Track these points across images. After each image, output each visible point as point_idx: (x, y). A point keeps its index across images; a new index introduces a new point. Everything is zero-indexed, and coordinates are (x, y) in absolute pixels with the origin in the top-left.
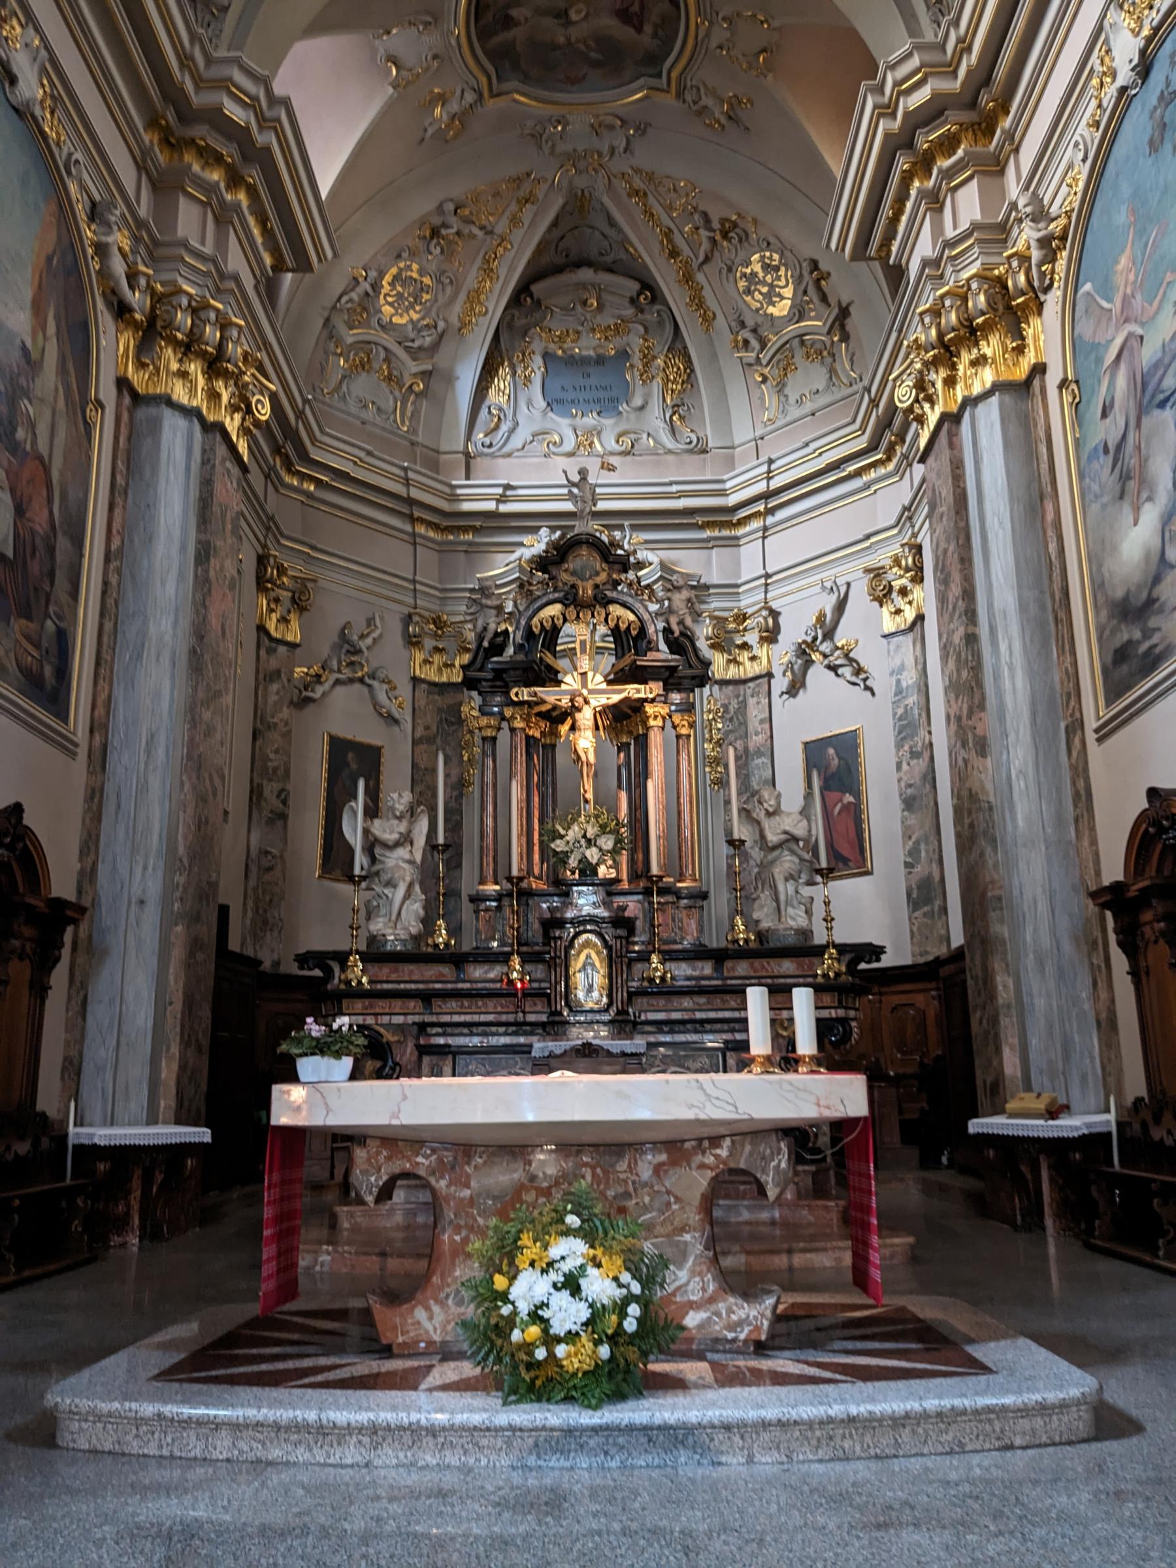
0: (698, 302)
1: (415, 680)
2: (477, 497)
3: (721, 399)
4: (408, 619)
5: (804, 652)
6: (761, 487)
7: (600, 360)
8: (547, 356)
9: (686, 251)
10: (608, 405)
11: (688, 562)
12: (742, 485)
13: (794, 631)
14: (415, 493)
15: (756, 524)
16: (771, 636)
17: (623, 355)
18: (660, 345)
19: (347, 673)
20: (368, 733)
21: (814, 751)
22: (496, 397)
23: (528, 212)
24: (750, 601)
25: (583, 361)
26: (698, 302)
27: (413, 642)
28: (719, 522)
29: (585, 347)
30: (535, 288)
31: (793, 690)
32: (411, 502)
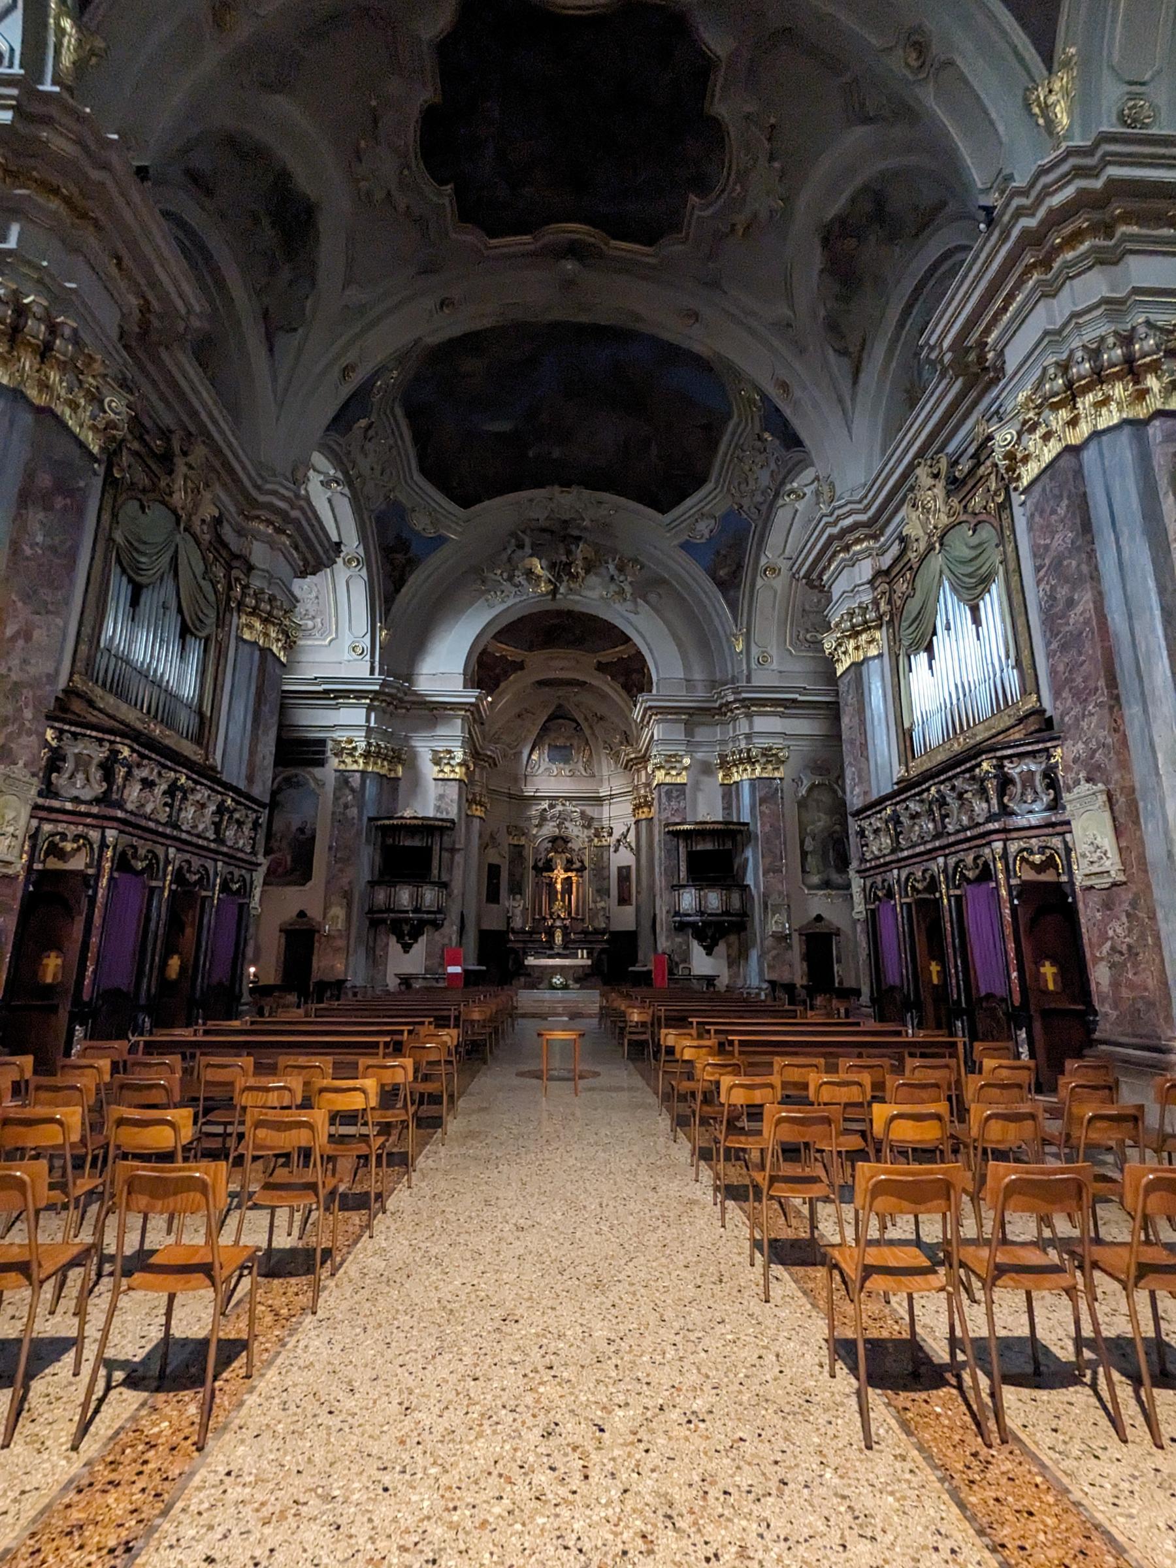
0: (593, 734)
2: (529, 791)
3: (600, 763)
5: (619, 841)
7: (565, 747)
10: (566, 760)
11: (589, 811)
12: (604, 792)
13: (617, 835)
16: (610, 834)
20: (495, 860)
21: (620, 869)
22: (534, 757)
24: (605, 823)
26: (593, 734)
27: (509, 833)
28: (598, 801)
31: (616, 851)
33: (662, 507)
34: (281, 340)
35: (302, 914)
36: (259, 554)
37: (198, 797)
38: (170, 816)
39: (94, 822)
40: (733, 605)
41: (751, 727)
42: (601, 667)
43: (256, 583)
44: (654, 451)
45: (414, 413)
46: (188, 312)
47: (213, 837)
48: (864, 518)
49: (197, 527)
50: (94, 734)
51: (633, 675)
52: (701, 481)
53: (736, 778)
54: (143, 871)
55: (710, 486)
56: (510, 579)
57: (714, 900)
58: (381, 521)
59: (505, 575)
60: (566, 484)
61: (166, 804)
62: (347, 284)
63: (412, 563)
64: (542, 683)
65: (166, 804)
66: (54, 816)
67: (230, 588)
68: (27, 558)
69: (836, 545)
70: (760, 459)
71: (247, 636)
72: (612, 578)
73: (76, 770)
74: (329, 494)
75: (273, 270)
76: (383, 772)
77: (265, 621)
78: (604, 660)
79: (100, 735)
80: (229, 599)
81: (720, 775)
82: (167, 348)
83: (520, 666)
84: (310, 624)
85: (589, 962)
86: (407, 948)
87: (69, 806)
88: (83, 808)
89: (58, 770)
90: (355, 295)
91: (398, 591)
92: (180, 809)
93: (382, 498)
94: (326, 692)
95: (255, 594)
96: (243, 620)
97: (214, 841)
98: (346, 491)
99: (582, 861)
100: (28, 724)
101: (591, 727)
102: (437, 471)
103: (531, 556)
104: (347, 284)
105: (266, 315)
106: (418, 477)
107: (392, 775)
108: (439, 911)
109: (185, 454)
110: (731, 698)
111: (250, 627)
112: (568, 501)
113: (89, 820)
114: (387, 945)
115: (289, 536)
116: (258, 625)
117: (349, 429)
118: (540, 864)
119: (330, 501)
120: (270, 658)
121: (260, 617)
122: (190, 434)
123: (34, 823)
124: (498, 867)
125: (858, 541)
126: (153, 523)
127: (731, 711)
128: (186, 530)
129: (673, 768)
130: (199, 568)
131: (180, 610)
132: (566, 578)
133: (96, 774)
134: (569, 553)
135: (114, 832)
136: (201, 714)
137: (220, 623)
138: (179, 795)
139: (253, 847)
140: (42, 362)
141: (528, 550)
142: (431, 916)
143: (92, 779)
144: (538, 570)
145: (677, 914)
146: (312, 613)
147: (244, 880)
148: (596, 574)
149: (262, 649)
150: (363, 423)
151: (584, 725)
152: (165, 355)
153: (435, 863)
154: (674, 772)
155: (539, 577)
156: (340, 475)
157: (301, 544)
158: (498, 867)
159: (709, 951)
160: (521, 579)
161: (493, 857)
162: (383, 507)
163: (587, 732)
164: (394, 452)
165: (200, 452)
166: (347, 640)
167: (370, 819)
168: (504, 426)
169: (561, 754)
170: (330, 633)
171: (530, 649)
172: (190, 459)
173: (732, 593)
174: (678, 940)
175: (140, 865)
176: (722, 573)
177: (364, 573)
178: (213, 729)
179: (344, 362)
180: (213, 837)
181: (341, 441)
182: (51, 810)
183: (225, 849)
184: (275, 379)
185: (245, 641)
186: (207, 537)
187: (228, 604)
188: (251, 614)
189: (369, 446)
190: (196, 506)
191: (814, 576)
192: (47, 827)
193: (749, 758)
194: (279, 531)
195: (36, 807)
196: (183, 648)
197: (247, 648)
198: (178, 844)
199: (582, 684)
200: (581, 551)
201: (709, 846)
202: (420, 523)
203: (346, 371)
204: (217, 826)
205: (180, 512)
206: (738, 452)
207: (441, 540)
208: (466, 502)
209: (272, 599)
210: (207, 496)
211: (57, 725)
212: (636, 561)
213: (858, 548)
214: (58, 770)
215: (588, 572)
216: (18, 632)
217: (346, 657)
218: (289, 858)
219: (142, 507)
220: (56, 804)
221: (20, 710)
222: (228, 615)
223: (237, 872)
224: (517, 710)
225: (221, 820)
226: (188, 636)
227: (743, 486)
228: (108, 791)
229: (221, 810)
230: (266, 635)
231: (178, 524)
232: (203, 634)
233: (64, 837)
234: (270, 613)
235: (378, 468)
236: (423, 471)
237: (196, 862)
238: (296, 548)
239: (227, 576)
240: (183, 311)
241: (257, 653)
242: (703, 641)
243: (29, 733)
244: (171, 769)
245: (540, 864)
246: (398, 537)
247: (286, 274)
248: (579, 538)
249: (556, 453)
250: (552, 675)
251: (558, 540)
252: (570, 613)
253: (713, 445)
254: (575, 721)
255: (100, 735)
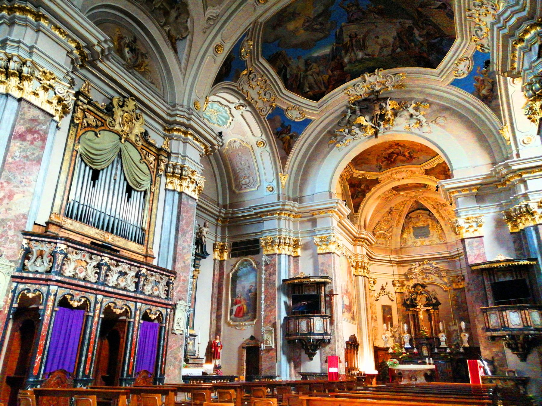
0: (441, 216)
1: (395, 292)
4: (393, 281)
6: (457, 253)
8: (413, 227)
9: (437, 208)
10: (426, 235)
14: (392, 259)
15: (458, 258)
17: (428, 225)
18: (435, 223)
19: (384, 293)
20: (388, 303)
23: (406, 206)
25: (421, 227)
29: (420, 224)
30: (409, 215)
32: (391, 261)
33: (433, 65)
34: (180, 45)
35: (252, 338)
36: (176, 147)
37: (120, 269)
38: (98, 279)
39: (44, 282)
40: (496, 110)
41: (526, 187)
42: (427, 172)
43: (173, 161)
44: (416, 32)
45: (272, 60)
46: (99, 42)
47: (134, 289)
48: (525, 14)
49: (133, 138)
50: (46, 240)
51: (444, 171)
52: (452, 39)
53: (521, 227)
54: (78, 308)
55: (458, 41)
56: (350, 132)
57: (514, 319)
58: (270, 118)
59: (347, 131)
60: (371, 71)
61: (96, 273)
62: (205, 7)
63: (294, 138)
64: (397, 189)
65: (96, 273)
66: (24, 281)
67: (158, 165)
68: (10, 163)
69: (511, 42)
70: (483, 10)
71: (170, 187)
72: (411, 116)
73: (37, 258)
74: (240, 112)
75: (167, 14)
76: (288, 254)
77: (181, 178)
78: (428, 167)
79: (49, 240)
80: (158, 170)
81: (510, 225)
82: (101, 61)
83: (376, 182)
84: (248, 181)
85: (433, 367)
86: (311, 357)
87: (31, 275)
88: (38, 276)
89: (28, 259)
90: (211, 11)
91: (288, 154)
92: (107, 276)
93: (268, 108)
94: (256, 214)
95: (173, 165)
96: (169, 180)
97: (134, 292)
98: (248, 108)
99: (435, 298)
100: (10, 238)
101: (438, 212)
102: (295, 85)
103: (361, 115)
104: (205, 7)
105: (169, 35)
106: (285, 91)
107: (295, 255)
108: (326, 333)
109: (122, 106)
110: (504, 171)
111: (171, 182)
112: (373, 81)
113: (41, 282)
114: (300, 355)
115: (191, 134)
116: (176, 181)
117: (238, 77)
118: (408, 302)
119: (242, 115)
120: (184, 196)
121: (177, 177)
122: (124, 97)
123: (15, 284)
124: (390, 308)
125: (526, 32)
126: (106, 141)
127: (509, 180)
128: (125, 141)
129: (470, 227)
130: (136, 157)
131: (125, 179)
132: (382, 123)
133: (46, 259)
134: (382, 108)
135: (56, 288)
136: (143, 230)
137: (153, 182)
138: (105, 268)
139: (167, 295)
140: (20, 80)
141: (358, 112)
142: (320, 337)
143: (44, 261)
144: (365, 123)
145: (488, 329)
146: (248, 175)
147: (161, 313)
148: (400, 116)
149: (180, 193)
150: (245, 72)
151: (434, 212)
152: (100, 65)
153: (323, 304)
154: (471, 230)
155: (366, 127)
156: (242, 101)
157: (198, 136)
158: (390, 308)
159: (523, 358)
160: (357, 130)
161: (385, 301)
162: (270, 112)
163: (437, 215)
164: (268, 82)
165: (131, 104)
166: (265, 185)
167: (283, 281)
168: (327, 51)
169: (422, 233)
170: (257, 182)
171: (380, 169)
172: (125, 108)
173: (493, 103)
174: (494, 350)
175: (75, 304)
176: (484, 92)
177: (268, 148)
178: (151, 236)
179: (214, 45)
180: (134, 289)
181: (234, 84)
182: (22, 278)
183: (141, 296)
184: (179, 63)
185: (170, 190)
186: (140, 143)
187: (157, 172)
188: (173, 176)
189: (253, 83)
190: (131, 129)
191: (509, 69)
192: (21, 286)
193: (528, 211)
194: (185, 133)
195: (13, 277)
196: (129, 197)
197: (171, 193)
198: (104, 293)
199: (425, 186)
200: (389, 106)
201: (509, 278)
202: (294, 115)
203: (217, 48)
204: (137, 284)
205: (121, 133)
206: (468, 14)
207: (307, 122)
208: (316, 97)
209: (182, 168)
210: (137, 124)
211: (28, 237)
212: (426, 101)
213: (528, 37)
214: (28, 259)
215: (395, 115)
216: (4, 197)
217: (266, 194)
218: (245, 307)
219: (96, 135)
220: (25, 275)
221: (6, 231)
222: (158, 179)
223: (154, 309)
224: (387, 209)
225: (139, 282)
226: (133, 192)
227: (479, 32)
228: (51, 268)
229: (138, 276)
230: (181, 185)
231: (121, 139)
232: (143, 189)
233: (29, 290)
234: (181, 174)
235: (262, 92)
236: (288, 87)
237: (120, 303)
238: (197, 140)
239: (157, 159)
240: (96, 42)
241: (177, 196)
242: (489, 140)
243: (12, 241)
244: (98, 255)
245: (408, 302)
246: (282, 125)
247: (173, 14)
248: (385, 99)
249: (360, 55)
250: (396, 184)
251: (370, 104)
252: (397, 144)
253: (451, 15)
254: (426, 209)
255: (49, 240)
